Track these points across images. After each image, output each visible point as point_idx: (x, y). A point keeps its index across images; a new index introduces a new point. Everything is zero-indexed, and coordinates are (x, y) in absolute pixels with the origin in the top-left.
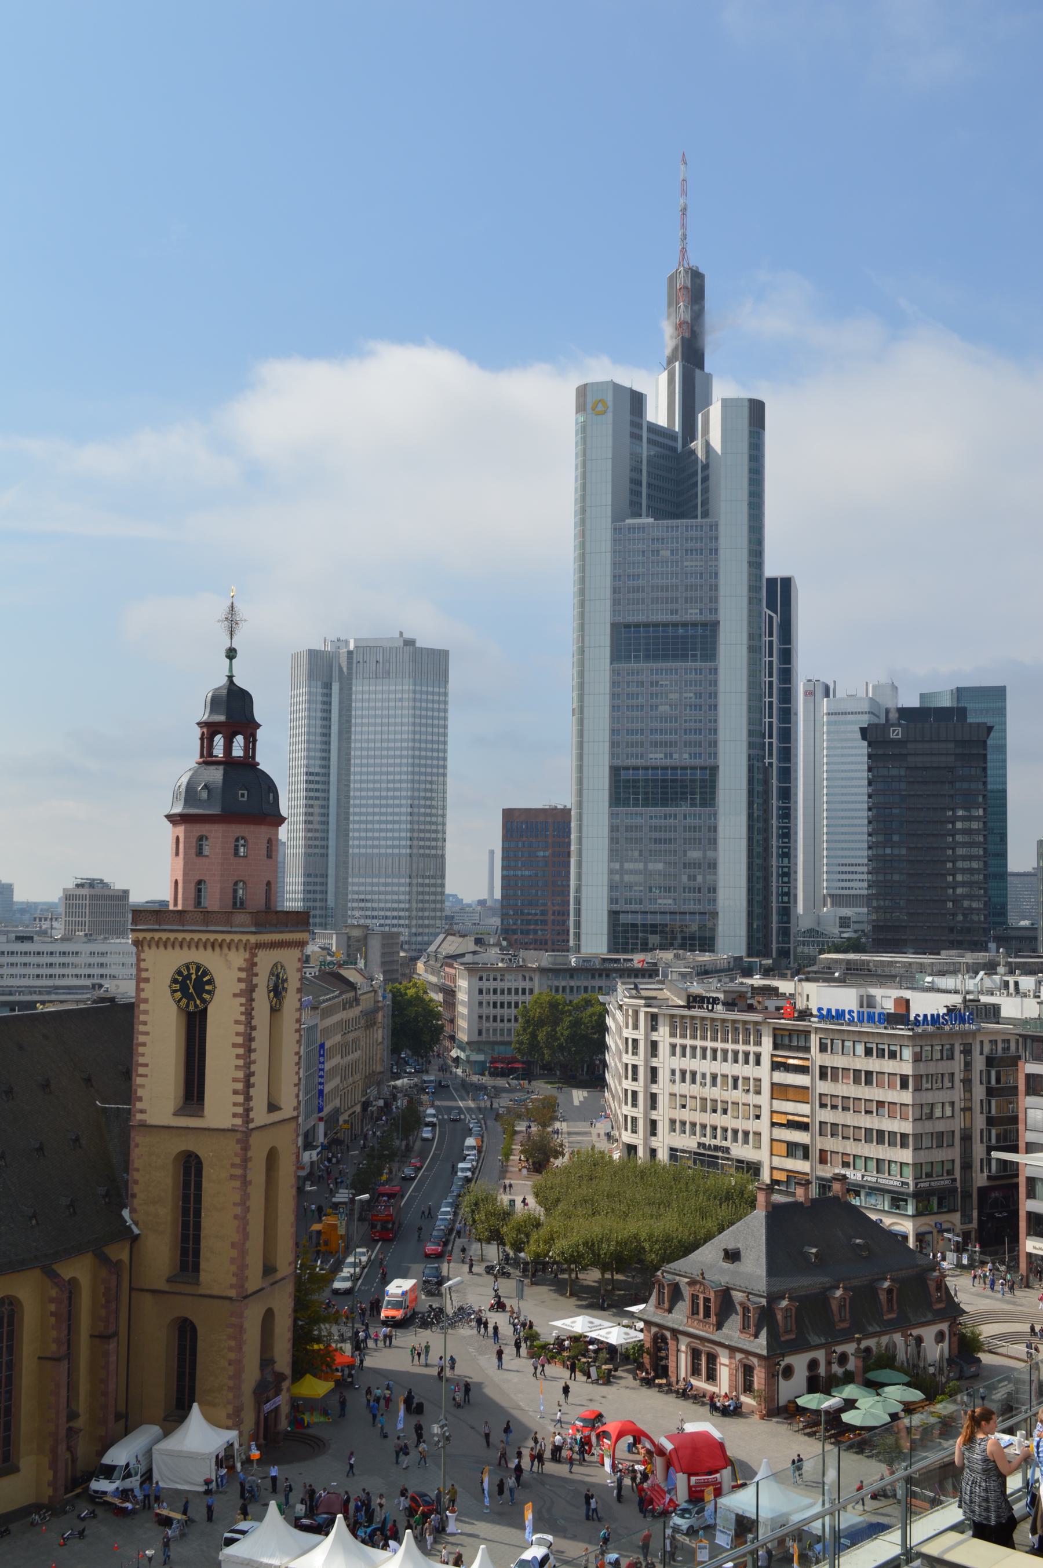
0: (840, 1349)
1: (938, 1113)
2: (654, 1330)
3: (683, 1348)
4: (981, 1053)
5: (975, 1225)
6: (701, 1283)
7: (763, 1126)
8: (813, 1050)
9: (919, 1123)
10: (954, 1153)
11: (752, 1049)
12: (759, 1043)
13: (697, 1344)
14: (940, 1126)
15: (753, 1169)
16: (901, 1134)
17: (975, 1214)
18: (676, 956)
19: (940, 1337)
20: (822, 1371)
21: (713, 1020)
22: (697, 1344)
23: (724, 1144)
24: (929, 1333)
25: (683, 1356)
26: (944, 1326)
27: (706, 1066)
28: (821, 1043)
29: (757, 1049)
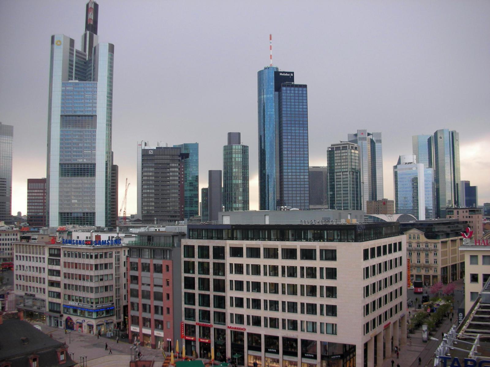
4: (125, 255)
5: (122, 319)
7: (46, 286)
8: (61, 256)
10: (113, 293)
11: (42, 256)
12: (44, 254)
14: (107, 283)
16: (91, 287)
17: (122, 316)
18: (74, 227)
21: (30, 245)
23: (33, 293)
28: (64, 253)
29: (44, 256)
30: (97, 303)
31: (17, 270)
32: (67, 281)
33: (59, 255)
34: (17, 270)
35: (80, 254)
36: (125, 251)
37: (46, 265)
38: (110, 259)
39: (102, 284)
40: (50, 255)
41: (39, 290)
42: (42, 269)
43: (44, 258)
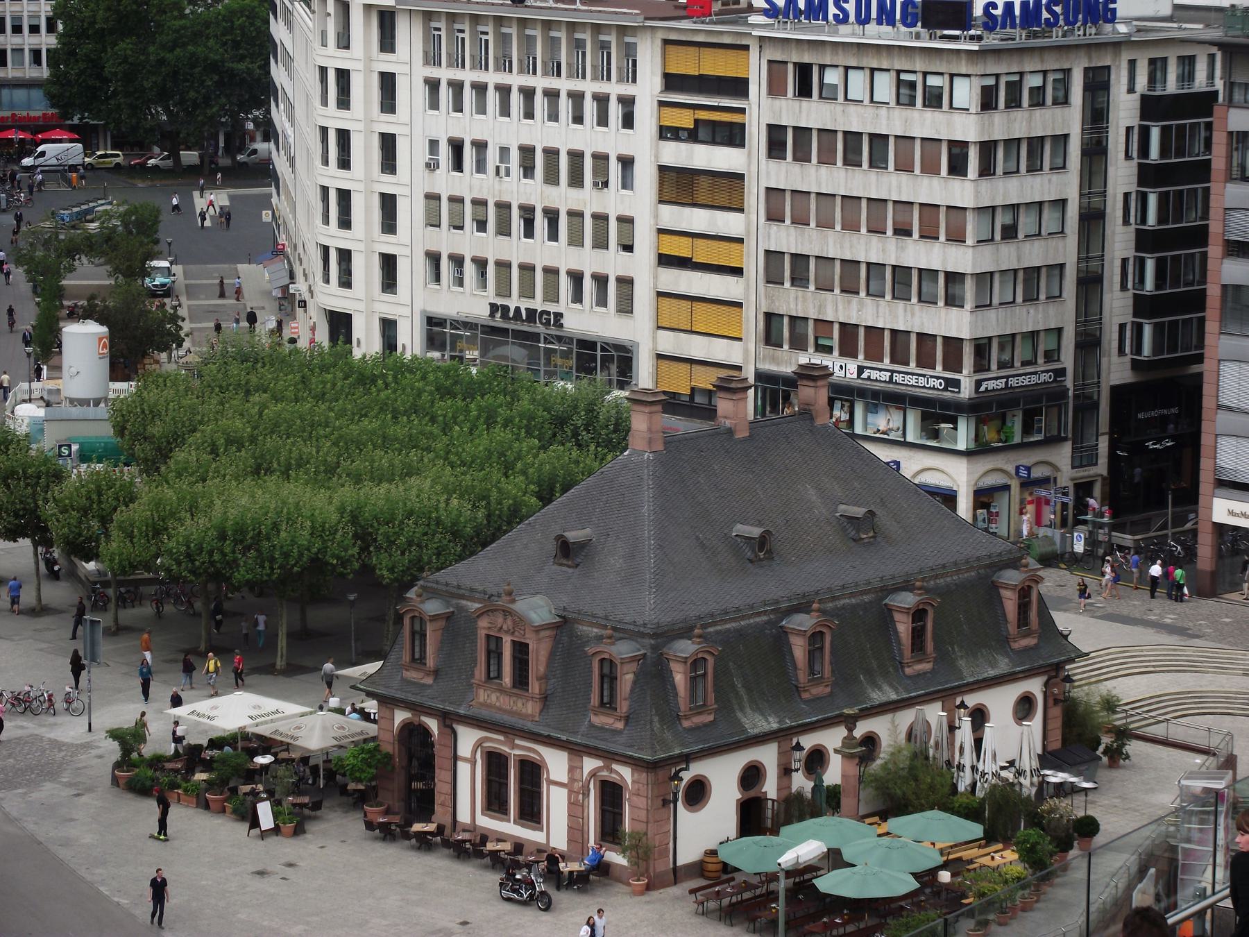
0: (808, 741)
1: (1026, 223)
2: (401, 716)
3: (465, 749)
4: (1131, 90)
5: (1102, 468)
6: (507, 613)
7: (641, 266)
8: (753, 89)
9: (987, 250)
11: (614, 89)
13: (498, 742)
14: (1034, 254)
15: (621, 359)
17: (1103, 445)
19: (1024, 707)
20: (770, 788)
21: (523, 23)
22: (498, 742)
23: (552, 308)
24: (1000, 702)
25: (464, 770)
26: (1035, 686)
27: (507, 132)
29: (627, 90)
30: (981, 363)
31: (432, 166)
32: (787, 239)
33: (738, 87)
34: (432, 166)
35: (804, 71)
36: (1132, 63)
37: (644, 146)
38: (1059, 111)
39: (1008, 256)
40: (672, 82)
41: (588, 284)
42: (614, 169)
43: (628, 103)
